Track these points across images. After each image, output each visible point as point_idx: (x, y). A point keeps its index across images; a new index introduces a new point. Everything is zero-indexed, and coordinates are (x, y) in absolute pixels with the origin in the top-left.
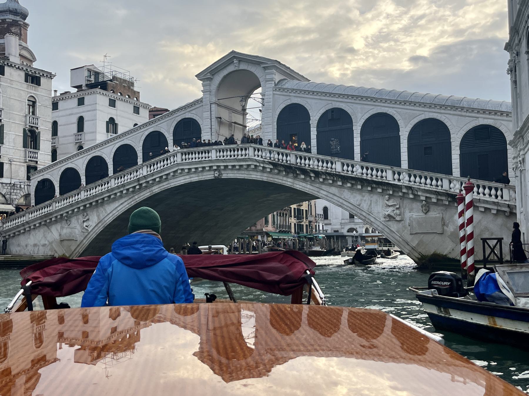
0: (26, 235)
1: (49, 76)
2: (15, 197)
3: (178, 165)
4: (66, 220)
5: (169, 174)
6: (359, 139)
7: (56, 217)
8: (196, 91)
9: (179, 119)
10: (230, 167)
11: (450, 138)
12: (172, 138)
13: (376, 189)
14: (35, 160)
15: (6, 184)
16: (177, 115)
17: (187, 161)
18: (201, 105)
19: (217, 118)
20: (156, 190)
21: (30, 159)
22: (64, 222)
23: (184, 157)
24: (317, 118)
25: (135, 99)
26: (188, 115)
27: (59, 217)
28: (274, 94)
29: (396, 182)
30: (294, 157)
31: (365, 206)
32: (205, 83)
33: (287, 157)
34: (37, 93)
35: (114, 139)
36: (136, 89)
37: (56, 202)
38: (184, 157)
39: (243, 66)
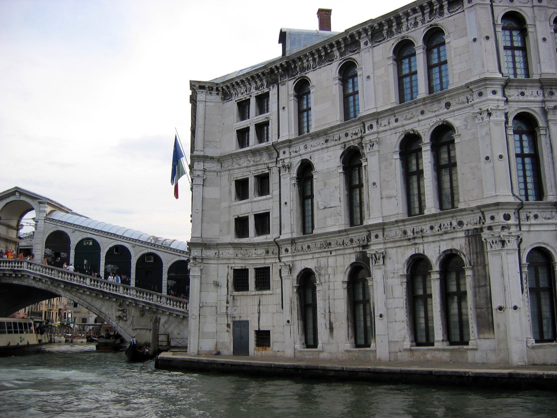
10: (8, 275)
11: (162, 267)
13: (112, 298)
24: (76, 243)
29: (125, 295)
31: (103, 310)
33: (52, 271)
39: (23, 198)
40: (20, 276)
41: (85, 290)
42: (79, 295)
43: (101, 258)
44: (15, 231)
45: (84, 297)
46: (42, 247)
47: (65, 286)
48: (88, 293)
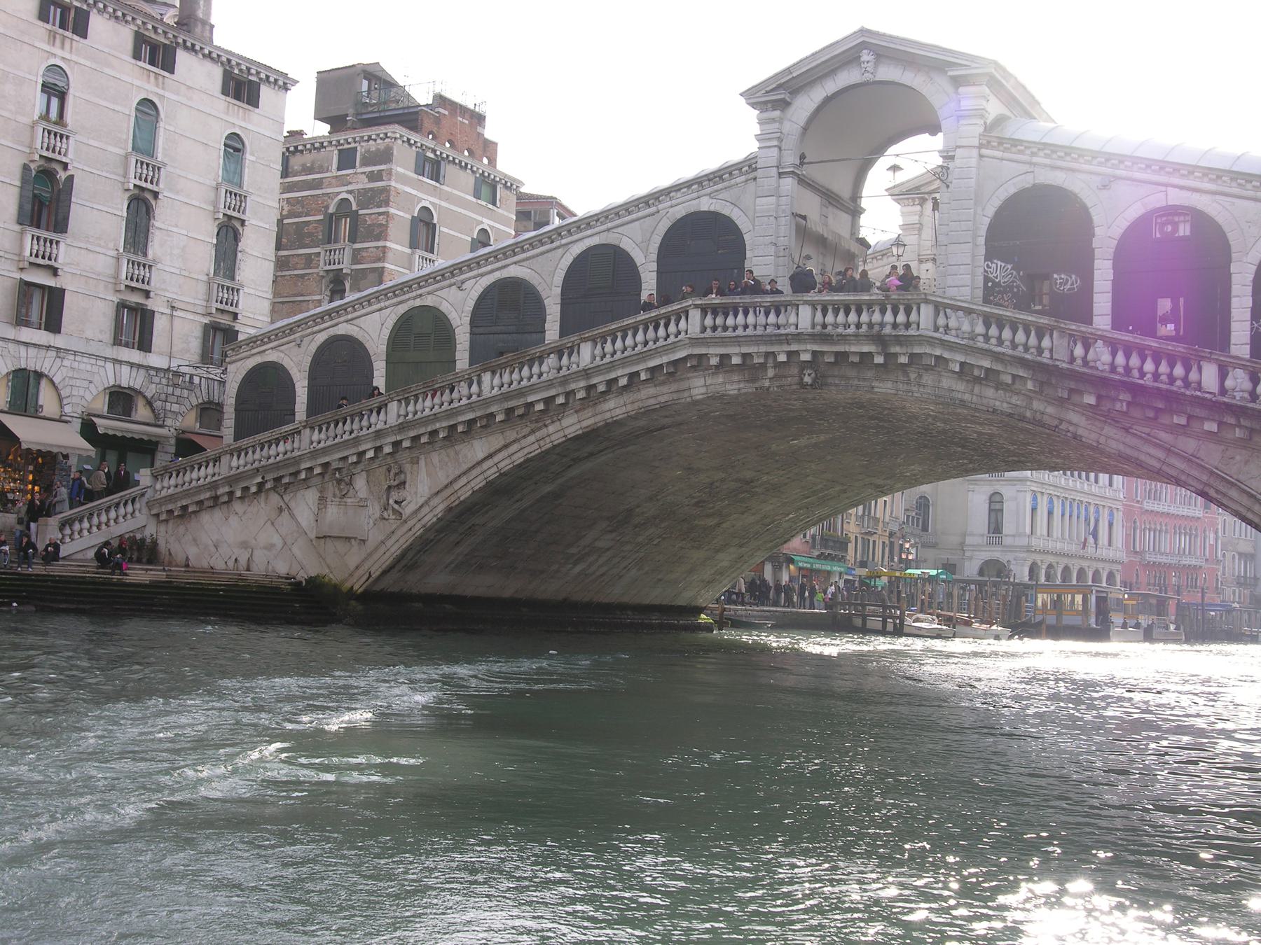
0: (218, 514)
1: (281, 83)
2: (175, 407)
3: (695, 342)
4: (339, 481)
5: (661, 366)
6: (1249, 302)
7: (310, 469)
8: (736, 136)
9: (680, 212)
10: (856, 359)
12: (654, 266)
14: (231, 309)
15: (158, 370)
16: (674, 202)
17: (719, 333)
18: (752, 175)
19: (795, 215)
20: (618, 411)
21: (219, 306)
22: (331, 488)
23: (709, 321)
25: (485, 161)
26: (705, 204)
27: (317, 471)
28: (981, 156)
30: (1065, 342)
32: (766, 115)
33: (1040, 338)
34: (249, 127)
35: (478, 263)
36: (490, 132)
37: (313, 428)
38: (709, 321)
39: (888, 73)
40: (903, 360)
41: (1198, 412)
42: (1164, 436)
43: (1236, 289)
44: (845, 218)
45: (1189, 445)
46: (974, 256)
47: (1099, 398)
48: (1212, 426)
